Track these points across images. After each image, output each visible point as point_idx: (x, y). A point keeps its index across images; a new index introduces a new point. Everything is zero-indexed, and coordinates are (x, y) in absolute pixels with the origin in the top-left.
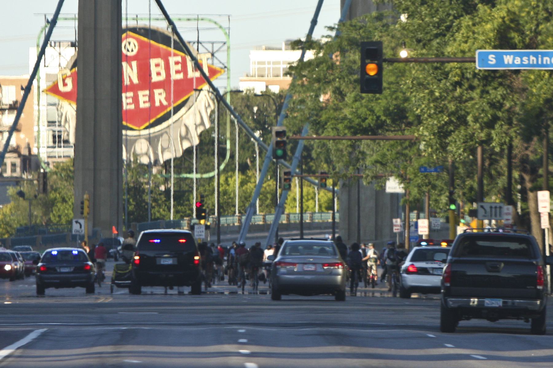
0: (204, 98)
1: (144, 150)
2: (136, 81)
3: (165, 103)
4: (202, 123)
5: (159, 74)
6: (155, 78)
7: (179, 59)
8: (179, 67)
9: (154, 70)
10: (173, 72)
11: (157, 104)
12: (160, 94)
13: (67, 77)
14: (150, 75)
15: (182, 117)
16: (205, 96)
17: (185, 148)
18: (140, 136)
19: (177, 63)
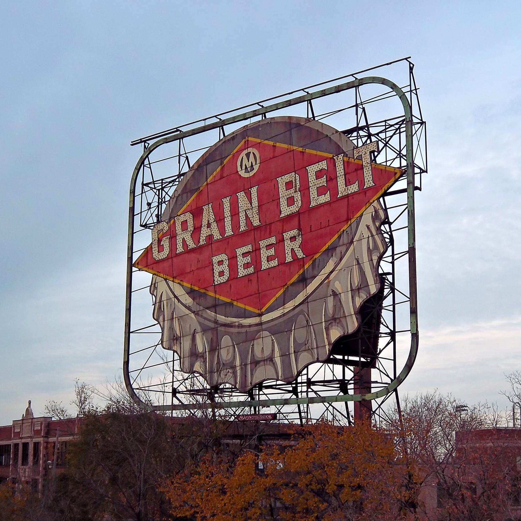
0: (367, 234)
1: (267, 353)
2: (256, 222)
3: (300, 255)
4: (364, 285)
5: (291, 201)
6: (286, 211)
7: (323, 165)
8: (323, 181)
9: (283, 193)
10: (313, 192)
11: (289, 259)
12: (293, 239)
13: (164, 235)
14: (278, 205)
15: (328, 277)
16: (368, 227)
17: (333, 340)
18: (261, 324)
19: (319, 175)
